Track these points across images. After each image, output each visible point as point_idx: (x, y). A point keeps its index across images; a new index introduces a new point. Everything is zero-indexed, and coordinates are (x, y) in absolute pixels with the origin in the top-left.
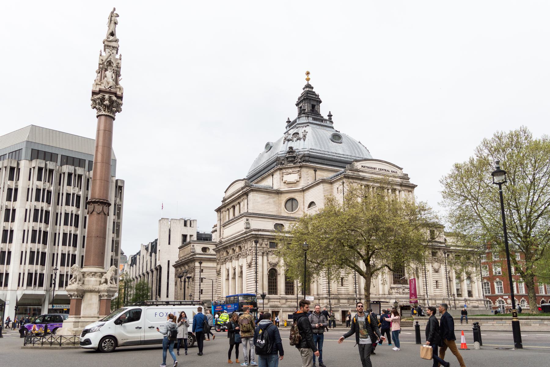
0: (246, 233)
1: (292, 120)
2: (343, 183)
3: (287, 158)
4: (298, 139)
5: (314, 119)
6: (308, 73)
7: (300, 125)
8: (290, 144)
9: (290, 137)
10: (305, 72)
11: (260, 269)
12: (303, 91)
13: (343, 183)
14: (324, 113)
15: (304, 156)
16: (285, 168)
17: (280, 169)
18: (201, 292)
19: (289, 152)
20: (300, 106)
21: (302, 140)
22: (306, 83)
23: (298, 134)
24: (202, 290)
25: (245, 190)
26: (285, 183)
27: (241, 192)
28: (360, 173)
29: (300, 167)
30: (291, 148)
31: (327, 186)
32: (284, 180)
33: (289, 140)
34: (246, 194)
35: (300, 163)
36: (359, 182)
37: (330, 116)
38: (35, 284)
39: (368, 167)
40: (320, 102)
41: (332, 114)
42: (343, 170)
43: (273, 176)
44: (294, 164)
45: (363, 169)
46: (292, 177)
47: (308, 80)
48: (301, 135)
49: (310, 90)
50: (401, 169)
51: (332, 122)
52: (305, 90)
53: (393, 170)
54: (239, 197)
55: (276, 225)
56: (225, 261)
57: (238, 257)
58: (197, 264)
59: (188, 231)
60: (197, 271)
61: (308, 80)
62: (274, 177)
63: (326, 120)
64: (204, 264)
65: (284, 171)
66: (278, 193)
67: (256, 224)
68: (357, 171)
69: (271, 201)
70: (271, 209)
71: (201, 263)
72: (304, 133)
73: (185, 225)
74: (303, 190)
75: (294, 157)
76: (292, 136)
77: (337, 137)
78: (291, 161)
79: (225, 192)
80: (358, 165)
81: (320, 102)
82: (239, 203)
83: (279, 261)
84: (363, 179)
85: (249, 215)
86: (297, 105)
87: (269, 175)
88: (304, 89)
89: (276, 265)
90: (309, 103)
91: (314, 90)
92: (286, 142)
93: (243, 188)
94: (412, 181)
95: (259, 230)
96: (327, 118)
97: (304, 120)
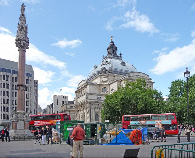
0: (86, 100)
1: (105, 56)
5: (114, 56)
6: (112, 37)
8: (104, 66)
9: (104, 63)
11: (92, 114)
14: (118, 54)
16: (102, 76)
19: (103, 69)
21: (109, 64)
28: (132, 78)
29: (108, 75)
30: (104, 67)
31: (119, 82)
33: (104, 64)
37: (121, 54)
38: (6, 118)
42: (125, 76)
44: (106, 74)
47: (112, 40)
48: (109, 63)
53: (146, 76)
54: (84, 87)
55: (98, 98)
57: (83, 110)
59: (64, 100)
61: (112, 40)
63: (119, 56)
66: (99, 85)
67: (90, 97)
68: (131, 76)
69: (97, 88)
70: (96, 92)
71: (69, 112)
73: (63, 98)
74: (109, 84)
78: (104, 73)
80: (131, 74)
82: (84, 89)
85: (87, 94)
86: (107, 50)
89: (98, 112)
90: (112, 50)
93: (85, 83)
94: (152, 81)
95: (91, 99)
97: (110, 56)
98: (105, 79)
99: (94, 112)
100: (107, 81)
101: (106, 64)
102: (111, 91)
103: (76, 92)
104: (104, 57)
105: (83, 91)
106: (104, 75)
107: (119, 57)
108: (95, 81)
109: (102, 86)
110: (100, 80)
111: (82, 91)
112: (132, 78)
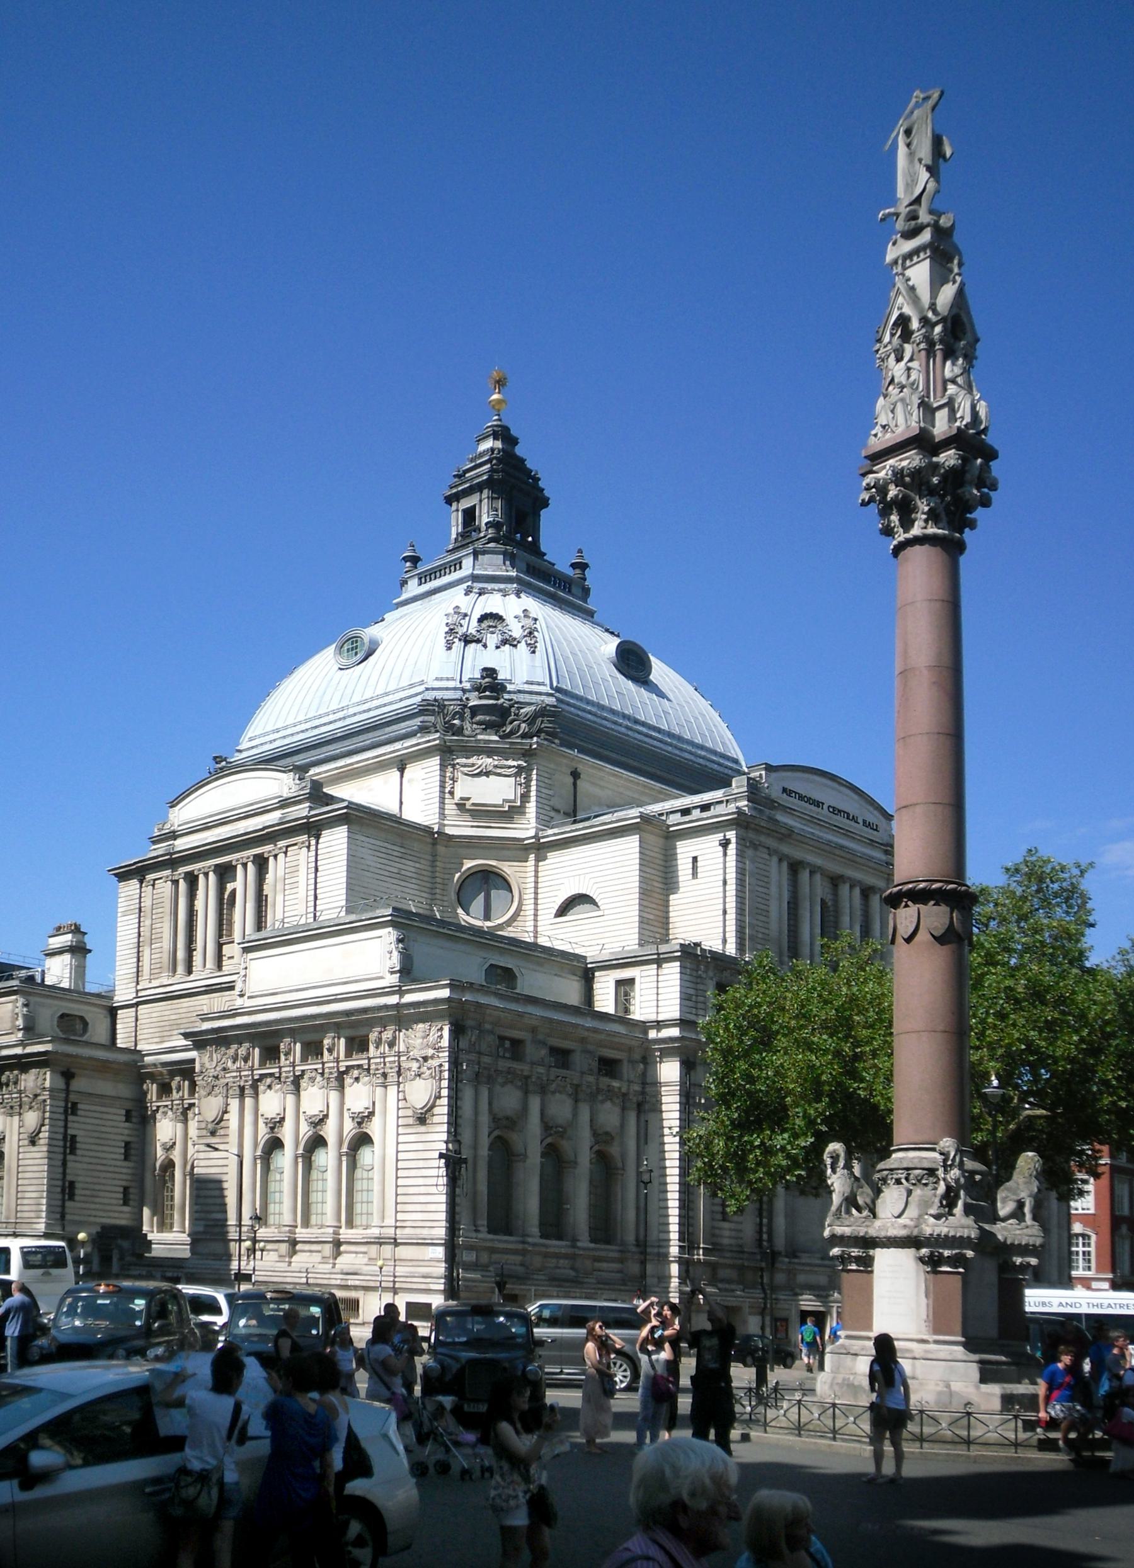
2: (725, 844)
3: (475, 710)
4: (505, 642)
7: (489, 586)
8: (478, 659)
9: (472, 627)
15: (543, 712)
19: (478, 688)
23: (498, 618)
24: (72, 1183)
25: (302, 811)
30: (490, 672)
32: (458, 794)
33: (467, 640)
35: (524, 736)
46: (497, 790)
50: (889, 817)
53: (871, 819)
69: (410, 867)
71: (68, 1076)
72: (528, 622)
78: (488, 726)
82: (261, 863)
92: (458, 645)
93: (284, 803)
98: (497, 790)
100: (510, 813)
101: (492, 640)
102: (564, 909)
105: (242, 884)
106: (490, 752)
108: (376, 792)
110: (445, 792)
111: (225, 873)
112: (781, 817)
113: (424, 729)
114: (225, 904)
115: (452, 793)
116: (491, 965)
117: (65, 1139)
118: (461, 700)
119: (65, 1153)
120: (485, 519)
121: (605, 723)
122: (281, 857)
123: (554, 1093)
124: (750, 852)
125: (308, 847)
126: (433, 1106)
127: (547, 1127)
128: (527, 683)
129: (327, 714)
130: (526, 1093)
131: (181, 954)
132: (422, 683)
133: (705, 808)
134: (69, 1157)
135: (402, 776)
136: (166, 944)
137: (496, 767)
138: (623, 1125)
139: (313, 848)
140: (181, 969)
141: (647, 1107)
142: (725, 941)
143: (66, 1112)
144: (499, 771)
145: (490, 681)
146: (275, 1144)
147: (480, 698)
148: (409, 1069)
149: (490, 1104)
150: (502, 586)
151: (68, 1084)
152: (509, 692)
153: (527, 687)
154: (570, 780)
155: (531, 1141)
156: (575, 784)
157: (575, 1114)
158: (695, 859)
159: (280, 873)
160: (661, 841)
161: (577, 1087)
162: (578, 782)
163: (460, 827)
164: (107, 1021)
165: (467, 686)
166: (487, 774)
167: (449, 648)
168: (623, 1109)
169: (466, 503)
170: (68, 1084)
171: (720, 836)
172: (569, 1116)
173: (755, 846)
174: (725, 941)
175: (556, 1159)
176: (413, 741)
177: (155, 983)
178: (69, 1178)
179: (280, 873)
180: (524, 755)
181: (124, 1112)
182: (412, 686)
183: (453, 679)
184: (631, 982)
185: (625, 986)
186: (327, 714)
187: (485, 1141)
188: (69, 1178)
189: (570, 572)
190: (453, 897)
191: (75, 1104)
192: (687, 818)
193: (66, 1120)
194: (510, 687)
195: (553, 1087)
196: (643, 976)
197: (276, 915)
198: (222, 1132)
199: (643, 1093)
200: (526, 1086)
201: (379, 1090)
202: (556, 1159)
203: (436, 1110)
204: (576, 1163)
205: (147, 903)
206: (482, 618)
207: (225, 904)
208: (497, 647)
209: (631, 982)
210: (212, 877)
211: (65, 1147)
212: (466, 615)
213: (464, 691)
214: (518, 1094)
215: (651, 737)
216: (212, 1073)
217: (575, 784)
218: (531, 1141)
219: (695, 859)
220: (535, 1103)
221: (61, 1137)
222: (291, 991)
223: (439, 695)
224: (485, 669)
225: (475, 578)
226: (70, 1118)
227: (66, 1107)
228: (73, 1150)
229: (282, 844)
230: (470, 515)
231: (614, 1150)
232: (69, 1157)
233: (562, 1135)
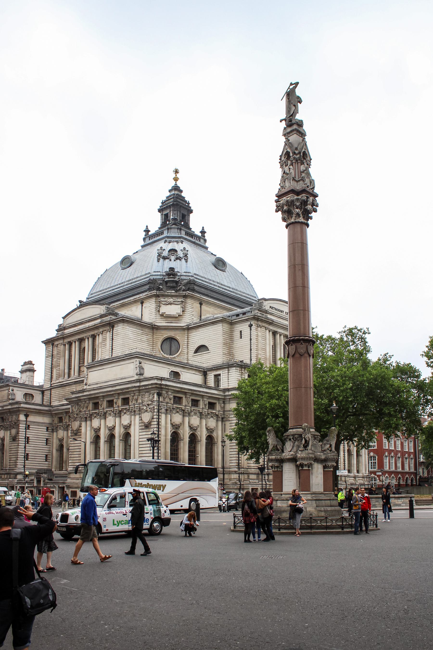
2: (251, 326)
3: (167, 282)
4: (177, 259)
6: (176, 172)
7: (173, 240)
9: (165, 254)
10: (173, 169)
12: (168, 194)
13: (251, 326)
14: (196, 229)
16: (163, 296)
17: (157, 296)
18: (26, 457)
19: (168, 275)
20: (165, 212)
21: (183, 260)
22: (173, 183)
23: (175, 251)
25: (107, 319)
26: (162, 315)
27: (99, 321)
28: (269, 316)
30: (172, 269)
31: (226, 326)
32: (162, 311)
33: (165, 258)
34: (111, 325)
35: (184, 291)
36: (267, 326)
37: (203, 232)
39: (276, 309)
40: (191, 212)
41: (205, 230)
43: (142, 303)
44: (176, 291)
45: (271, 311)
47: (176, 179)
49: (179, 193)
51: (205, 241)
52: (173, 192)
54: (96, 327)
56: (90, 417)
58: (22, 417)
60: (22, 426)
61: (176, 179)
62: (144, 305)
63: (197, 236)
64: (31, 418)
65: (162, 300)
66: (153, 328)
68: (266, 312)
69: (145, 338)
71: (27, 416)
75: (177, 282)
76: (167, 252)
77: (220, 264)
78: (172, 288)
79: (64, 318)
81: (191, 212)
82: (94, 337)
83: (183, 421)
84: (271, 323)
86: (159, 211)
87: (135, 302)
88: (170, 191)
90: (176, 210)
91: (183, 194)
92: (161, 260)
93: (102, 316)
96: (200, 234)
97: (174, 233)
99: (169, 426)
100: (178, 317)
101: (173, 258)
103: (49, 342)
104: (147, 231)
105: (87, 344)
106: (172, 296)
107: (199, 240)
109: (163, 332)
111: (81, 340)
113: (150, 289)
114: (82, 351)
115: (159, 311)
116: (172, 371)
117: (25, 438)
118: (162, 279)
119: (25, 444)
120: (171, 217)
121: (211, 285)
122: (100, 335)
123: (192, 416)
124: (259, 328)
125: (110, 331)
126: (151, 422)
127: (191, 427)
128: (185, 272)
129: (117, 285)
130: (184, 416)
131: (66, 371)
132: (149, 273)
133: (244, 314)
134: (27, 445)
135: (142, 306)
136: (61, 367)
137: (174, 301)
138: (217, 426)
139: (111, 332)
140: (66, 376)
141: (225, 419)
142: (251, 360)
143: (26, 429)
144: (175, 303)
145: (172, 272)
146: (97, 438)
147: (169, 278)
148: (143, 409)
149: (171, 420)
150: (177, 240)
151: (26, 419)
152: (179, 276)
153: (185, 274)
154: (199, 305)
155: (185, 433)
156: (201, 307)
157: (201, 423)
158: (241, 331)
159: (100, 341)
160: (229, 326)
161: (201, 413)
162: (202, 306)
163: (161, 323)
164: (41, 395)
165: (165, 274)
166: (171, 304)
167: (158, 261)
168: (217, 421)
169: (165, 212)
170: (26, 419)
171: (249, 323)
172: (198, 424)
173: (261, 327)
174: (251, 360)
175: (193, 439)
176: (146, 293)
177: (58, 381)
178: (26, 452)
179: (100, 341)
180: (183, 297)
181: (46, 428)
182: (146, 274)
183: (160, 272)
184: (219, 375)
185: (217, 377)
186: (117, 285)
187: (169, 434)
188: (26, 452)
189: (200, 234)
190: (160, 347)
191: (29, 426)
192: (238, 317)
193: (26, 432)
194: (179, 274)
195: (193, 413)
196: (223, 373)
197: (100, 356)
198: (79, 434)
199: (224, 414)
200: (184, 413)
201: (133, 417)
202: (193, 439)
203: (153, 423)
204: (201, 440)
205: (55, 353)
206: (170, 250)
207: (82, 351)
208: (175, 261)
209: (219, 375)
210: (77, 343)
211: (25, 441)
212: (164, 250)
213: (163, 275)
214: (181, 417)
215: (227, 290)
216: (76, 413)
217: (201, 307)
218: (185, 433)
219: (241, 331)
220: (187, 419)
221: (24, 438)
222: (103, 383)
223: (155, 277)
224: (170, 268)
225: (168, 237)
226: (27, 431)
227: (26, 427)
228: (28, 442)
229: (101, 330)
230: (166, 216)
231: (214, 435)
232: (27, 445)
233: (195, 430)
